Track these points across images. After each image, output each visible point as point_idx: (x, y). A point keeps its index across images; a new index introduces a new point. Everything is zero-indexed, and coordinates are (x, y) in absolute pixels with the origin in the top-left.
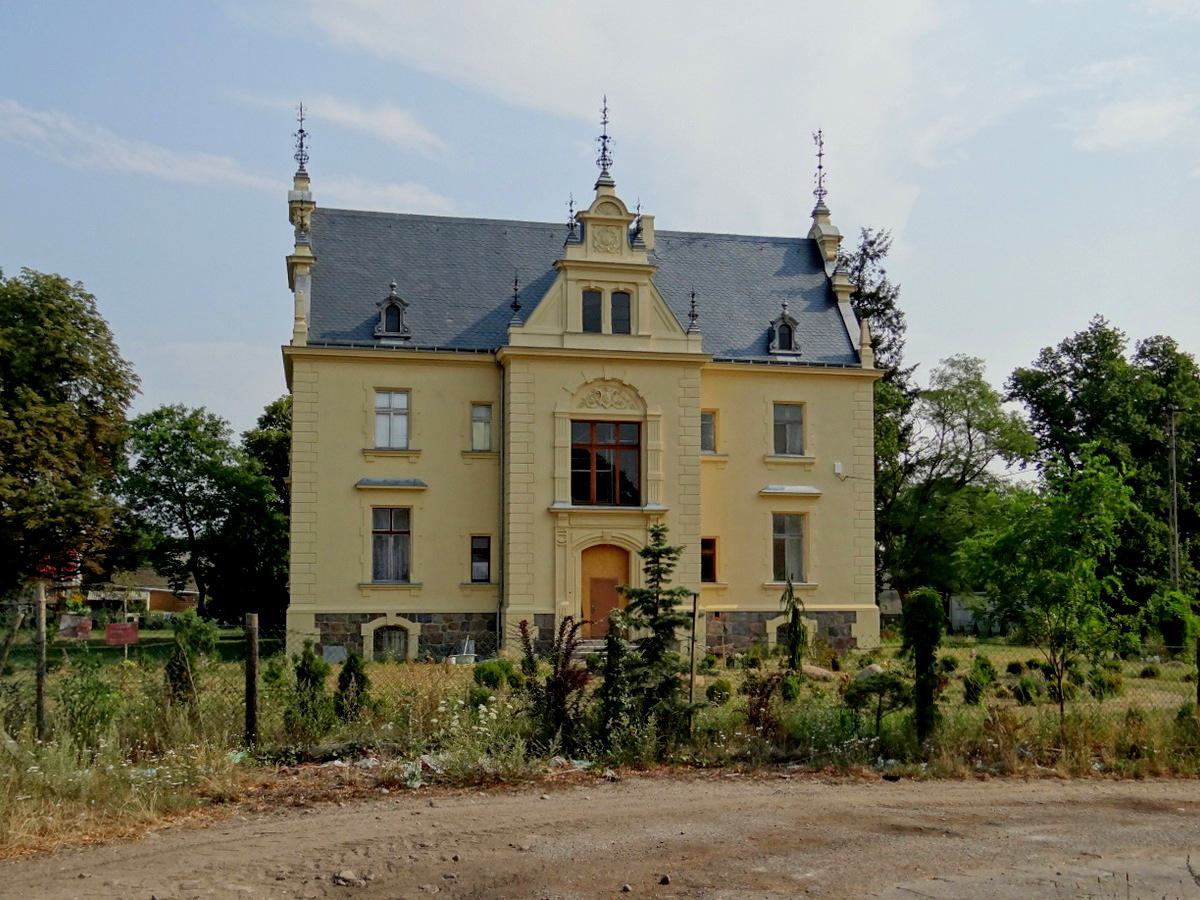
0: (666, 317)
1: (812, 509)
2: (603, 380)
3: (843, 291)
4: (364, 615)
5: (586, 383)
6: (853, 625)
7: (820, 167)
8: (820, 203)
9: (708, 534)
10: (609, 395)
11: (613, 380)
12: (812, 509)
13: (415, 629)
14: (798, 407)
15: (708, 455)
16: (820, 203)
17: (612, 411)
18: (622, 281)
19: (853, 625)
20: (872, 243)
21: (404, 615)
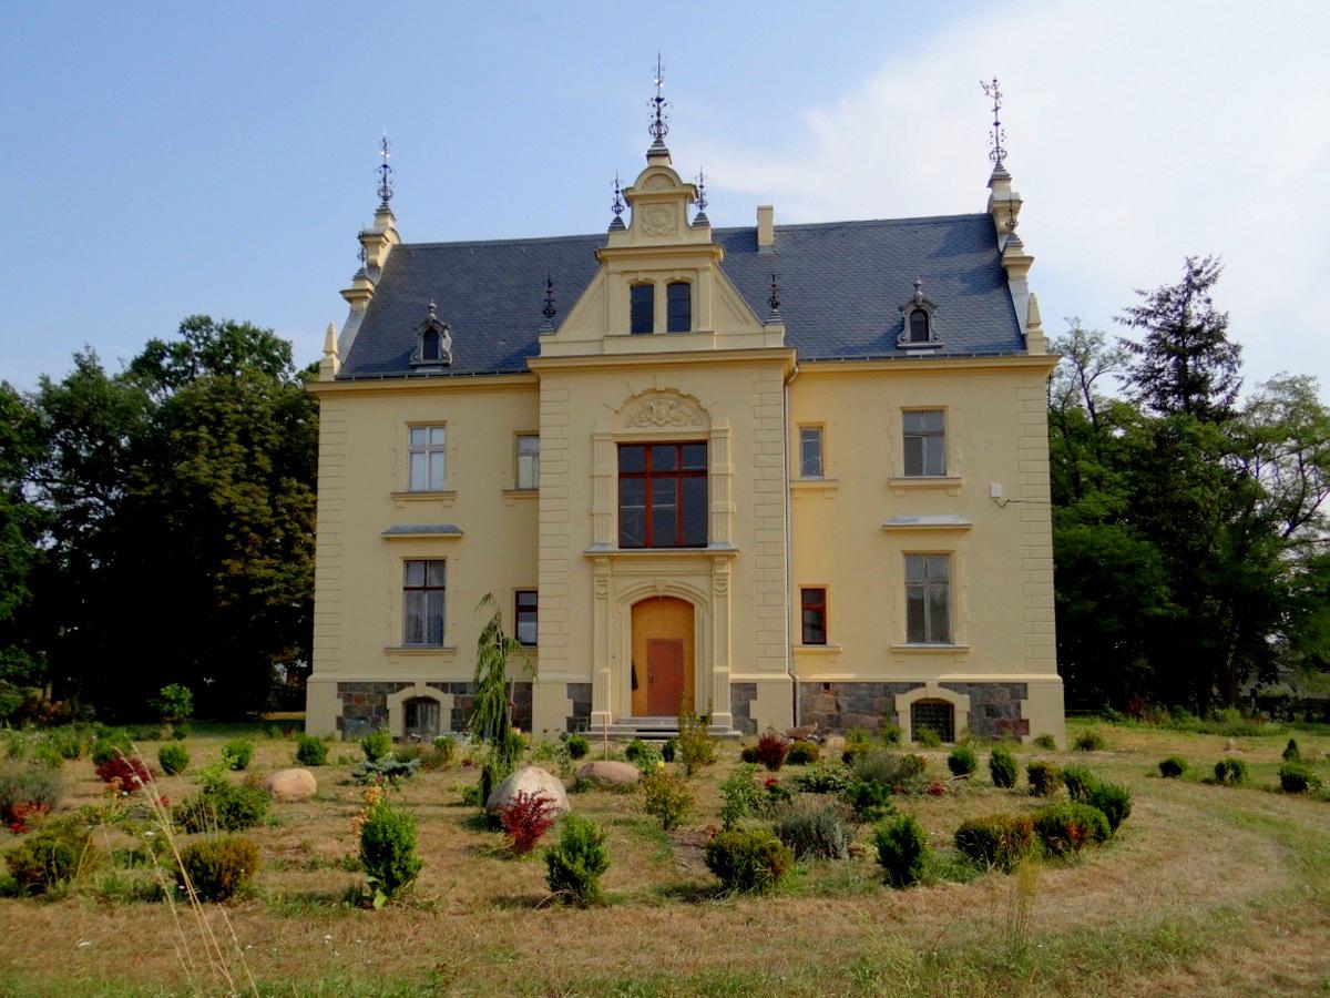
0: (739, 310)
1: (958, 545)
2: (655, 391)
3: (1014, 266)
4: (390, 685)
5: (633, 397)
6: (1023, 702)
7: (997, 124)
8: (999, 167)
9: (814, 582)
10: (663, 410)
11: (667, 390)
12: (958, 545)
13: (447, 701)
14: (938, 412)
15: (813, 482)
16: (999, 167)
17: (669, 429)
18: (678, 269)
19: (1023, 702)
20: (1198, 273)
21: (435, 685)
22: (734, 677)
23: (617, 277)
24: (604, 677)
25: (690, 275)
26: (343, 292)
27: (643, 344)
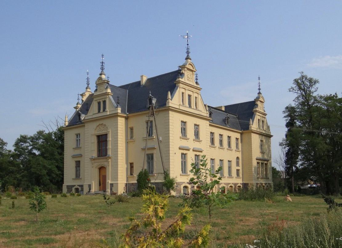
3: (177, 83)
7: (188, 45)
8: (188, 56)
22: (110, 182)
23: (95, 101)
24: (92, 183)
25: (105, 99)
26: (74, 107)
27: (100, 115)
